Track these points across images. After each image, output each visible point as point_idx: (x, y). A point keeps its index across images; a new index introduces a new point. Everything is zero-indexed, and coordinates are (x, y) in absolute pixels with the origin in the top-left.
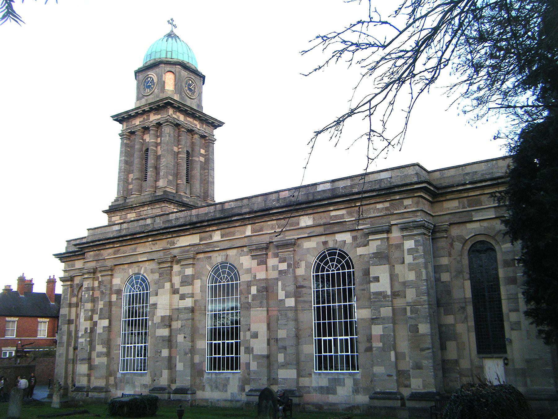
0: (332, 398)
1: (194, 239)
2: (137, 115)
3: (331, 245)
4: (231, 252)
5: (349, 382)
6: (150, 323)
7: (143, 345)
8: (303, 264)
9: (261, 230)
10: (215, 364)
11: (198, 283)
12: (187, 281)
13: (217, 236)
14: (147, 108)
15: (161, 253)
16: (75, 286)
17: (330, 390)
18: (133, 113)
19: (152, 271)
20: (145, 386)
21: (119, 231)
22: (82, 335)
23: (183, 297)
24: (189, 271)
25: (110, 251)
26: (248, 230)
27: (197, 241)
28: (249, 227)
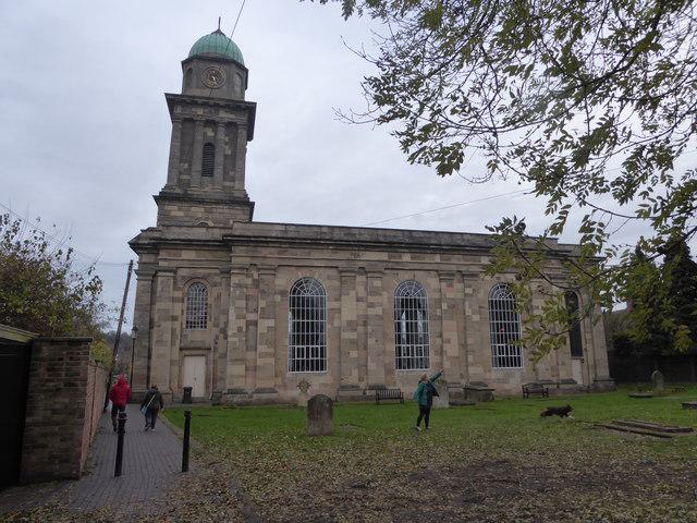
0: (506, 387)
1: (384, 256)
2: (204, 105)
3: (503, 280)
4: (419, 274)
5: (518, 374)
6: (328, 326)
7: (319, 347)
8: (482, 291)
9: (449, 260)
10: (297, 366)
11: (385, 294)
12: (375, 292)
13: (407, 257)
14: (222, 103)
15: (344, 262)
16: (179, 279)
17: (505, 381)
18: (200, 101)
19: (329, 278)
20: (326, 385)
21: (286, 231)
22: (234, 335)
23: (371, 305)
24: (377, 283)
25: (272, 250)
26: (437, 258)
27: (387, 258)
28: (438, 256)
